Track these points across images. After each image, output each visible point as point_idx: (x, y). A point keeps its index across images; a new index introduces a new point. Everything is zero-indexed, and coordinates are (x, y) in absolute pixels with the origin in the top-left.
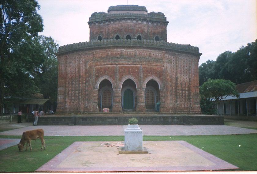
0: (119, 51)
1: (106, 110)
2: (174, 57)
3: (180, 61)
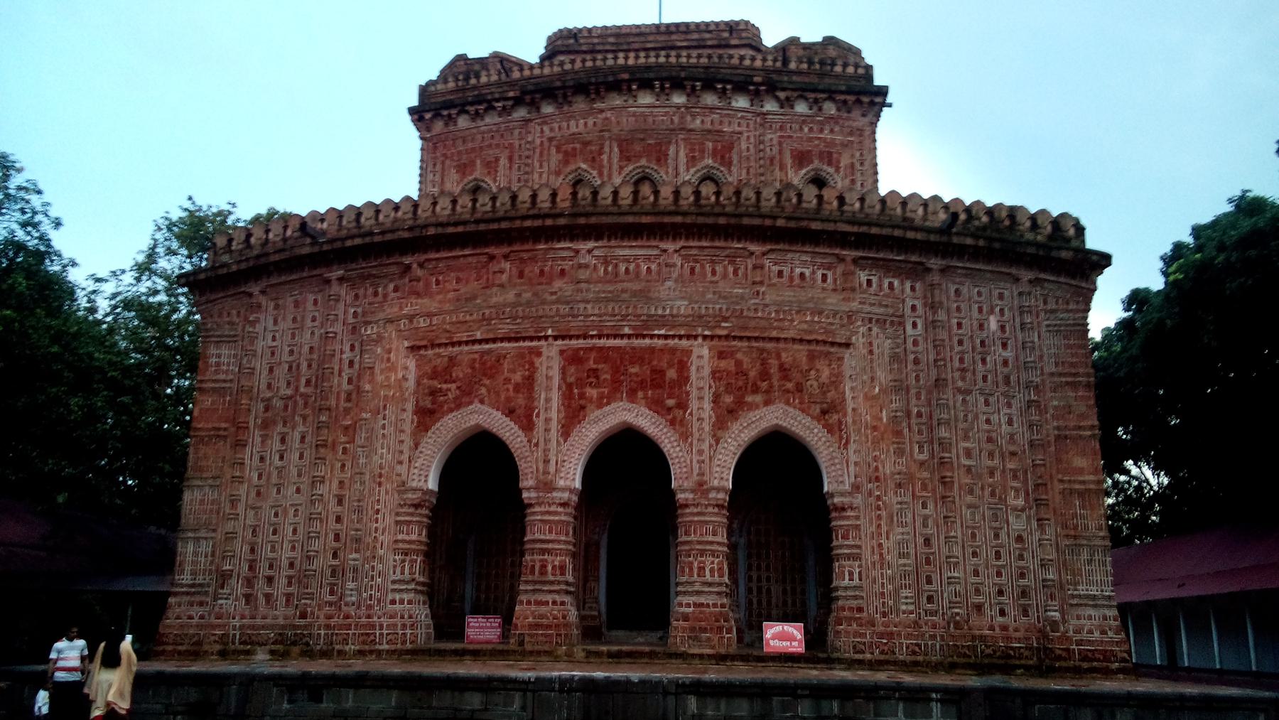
0: (565, 254)
1: (481, 629)
2: (918, 286)
3: (958, 309)
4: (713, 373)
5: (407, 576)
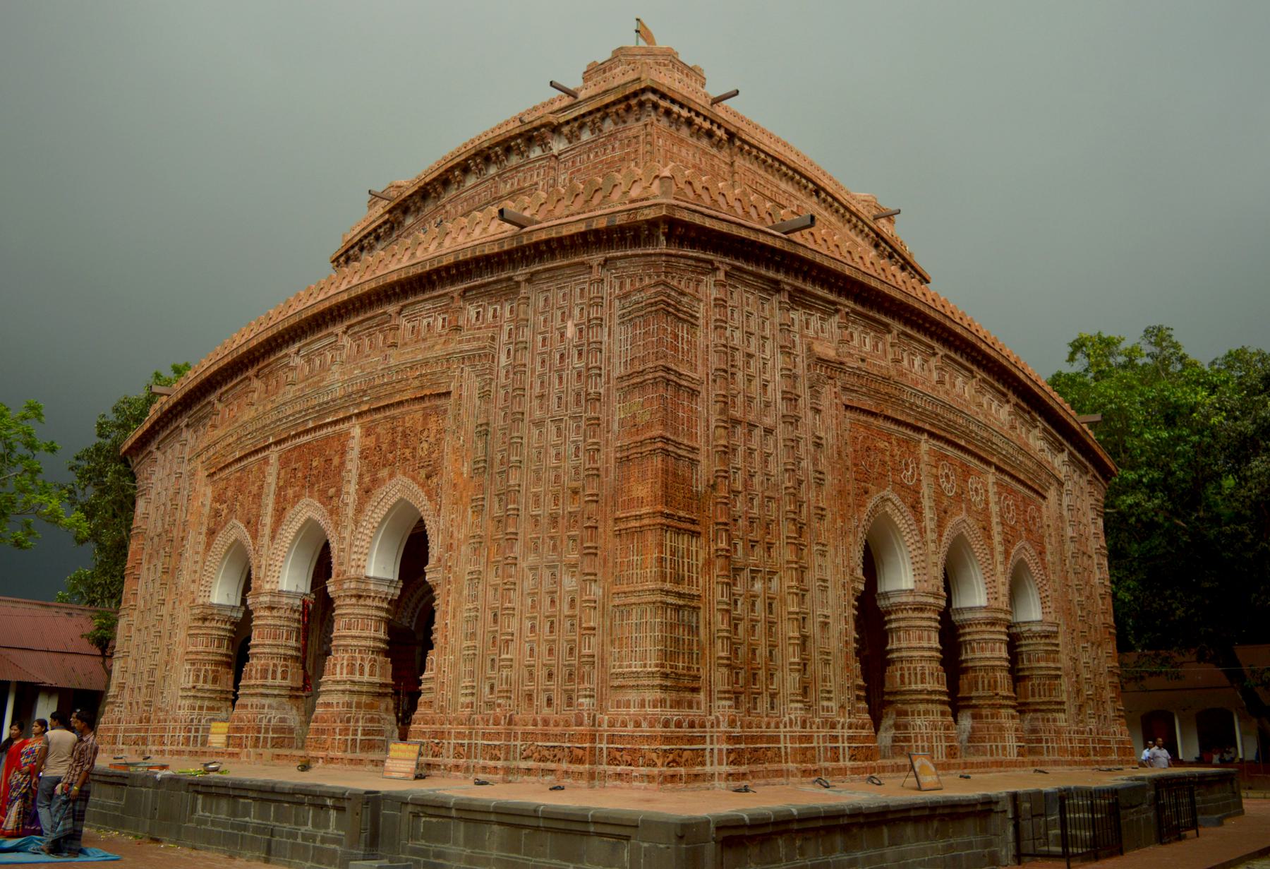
4: (361, 453)
5: (190, 685)
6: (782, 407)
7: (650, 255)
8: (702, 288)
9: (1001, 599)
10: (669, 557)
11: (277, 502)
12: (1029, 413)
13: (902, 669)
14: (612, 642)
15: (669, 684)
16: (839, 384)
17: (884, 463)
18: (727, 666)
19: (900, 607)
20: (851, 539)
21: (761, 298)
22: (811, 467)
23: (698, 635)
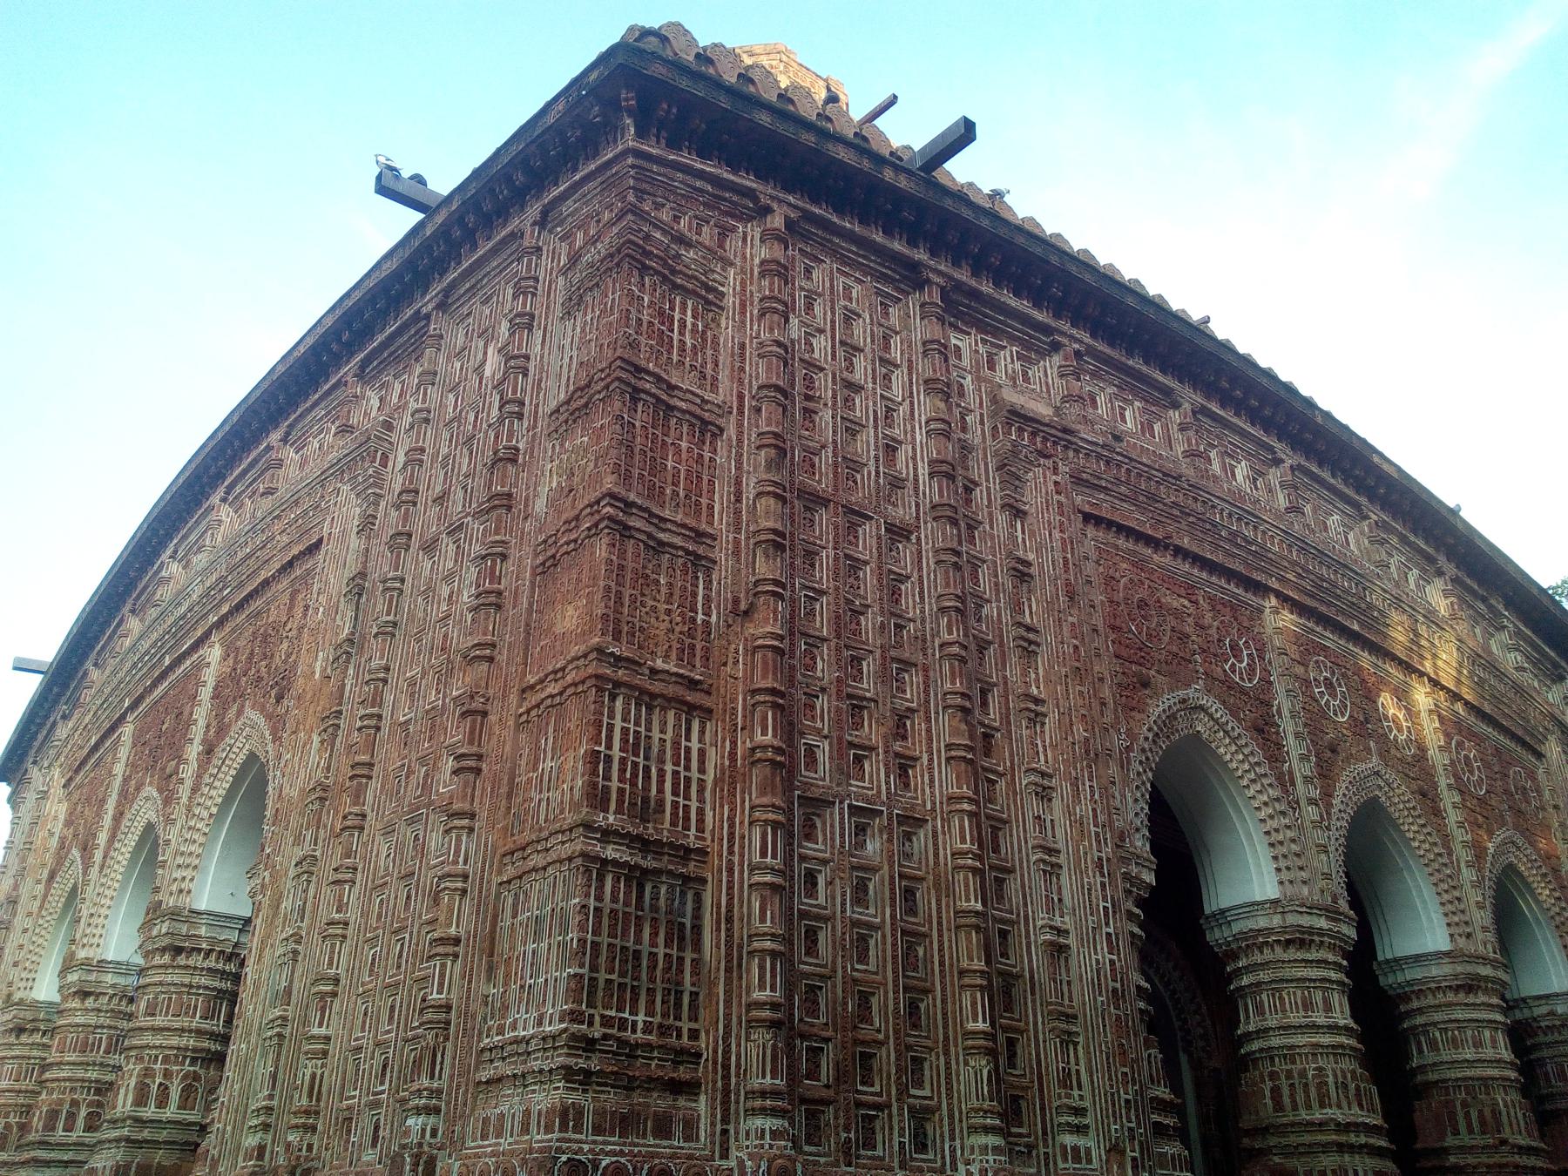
4: (215, 688)
6: (931, 490)
7: (609, 164)
8: (733, 245)
9: (1480, 936)
10: (616, 753)
11: (119, 804)
12: (1484, 600)
13: (1273, 1076)
14: (491, 970)
15: (594, 1065)
16: (1062, 468)
17: (1183, 637)
18: (774, 1025)
19: (1254, 941)
20: (1113, 770)
21: (879, 292)
22: (1006, 618)
23: (697, 945)
